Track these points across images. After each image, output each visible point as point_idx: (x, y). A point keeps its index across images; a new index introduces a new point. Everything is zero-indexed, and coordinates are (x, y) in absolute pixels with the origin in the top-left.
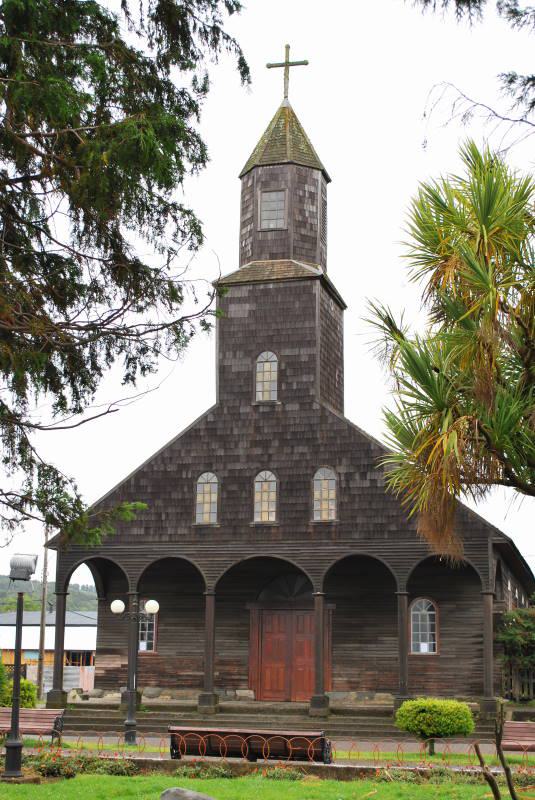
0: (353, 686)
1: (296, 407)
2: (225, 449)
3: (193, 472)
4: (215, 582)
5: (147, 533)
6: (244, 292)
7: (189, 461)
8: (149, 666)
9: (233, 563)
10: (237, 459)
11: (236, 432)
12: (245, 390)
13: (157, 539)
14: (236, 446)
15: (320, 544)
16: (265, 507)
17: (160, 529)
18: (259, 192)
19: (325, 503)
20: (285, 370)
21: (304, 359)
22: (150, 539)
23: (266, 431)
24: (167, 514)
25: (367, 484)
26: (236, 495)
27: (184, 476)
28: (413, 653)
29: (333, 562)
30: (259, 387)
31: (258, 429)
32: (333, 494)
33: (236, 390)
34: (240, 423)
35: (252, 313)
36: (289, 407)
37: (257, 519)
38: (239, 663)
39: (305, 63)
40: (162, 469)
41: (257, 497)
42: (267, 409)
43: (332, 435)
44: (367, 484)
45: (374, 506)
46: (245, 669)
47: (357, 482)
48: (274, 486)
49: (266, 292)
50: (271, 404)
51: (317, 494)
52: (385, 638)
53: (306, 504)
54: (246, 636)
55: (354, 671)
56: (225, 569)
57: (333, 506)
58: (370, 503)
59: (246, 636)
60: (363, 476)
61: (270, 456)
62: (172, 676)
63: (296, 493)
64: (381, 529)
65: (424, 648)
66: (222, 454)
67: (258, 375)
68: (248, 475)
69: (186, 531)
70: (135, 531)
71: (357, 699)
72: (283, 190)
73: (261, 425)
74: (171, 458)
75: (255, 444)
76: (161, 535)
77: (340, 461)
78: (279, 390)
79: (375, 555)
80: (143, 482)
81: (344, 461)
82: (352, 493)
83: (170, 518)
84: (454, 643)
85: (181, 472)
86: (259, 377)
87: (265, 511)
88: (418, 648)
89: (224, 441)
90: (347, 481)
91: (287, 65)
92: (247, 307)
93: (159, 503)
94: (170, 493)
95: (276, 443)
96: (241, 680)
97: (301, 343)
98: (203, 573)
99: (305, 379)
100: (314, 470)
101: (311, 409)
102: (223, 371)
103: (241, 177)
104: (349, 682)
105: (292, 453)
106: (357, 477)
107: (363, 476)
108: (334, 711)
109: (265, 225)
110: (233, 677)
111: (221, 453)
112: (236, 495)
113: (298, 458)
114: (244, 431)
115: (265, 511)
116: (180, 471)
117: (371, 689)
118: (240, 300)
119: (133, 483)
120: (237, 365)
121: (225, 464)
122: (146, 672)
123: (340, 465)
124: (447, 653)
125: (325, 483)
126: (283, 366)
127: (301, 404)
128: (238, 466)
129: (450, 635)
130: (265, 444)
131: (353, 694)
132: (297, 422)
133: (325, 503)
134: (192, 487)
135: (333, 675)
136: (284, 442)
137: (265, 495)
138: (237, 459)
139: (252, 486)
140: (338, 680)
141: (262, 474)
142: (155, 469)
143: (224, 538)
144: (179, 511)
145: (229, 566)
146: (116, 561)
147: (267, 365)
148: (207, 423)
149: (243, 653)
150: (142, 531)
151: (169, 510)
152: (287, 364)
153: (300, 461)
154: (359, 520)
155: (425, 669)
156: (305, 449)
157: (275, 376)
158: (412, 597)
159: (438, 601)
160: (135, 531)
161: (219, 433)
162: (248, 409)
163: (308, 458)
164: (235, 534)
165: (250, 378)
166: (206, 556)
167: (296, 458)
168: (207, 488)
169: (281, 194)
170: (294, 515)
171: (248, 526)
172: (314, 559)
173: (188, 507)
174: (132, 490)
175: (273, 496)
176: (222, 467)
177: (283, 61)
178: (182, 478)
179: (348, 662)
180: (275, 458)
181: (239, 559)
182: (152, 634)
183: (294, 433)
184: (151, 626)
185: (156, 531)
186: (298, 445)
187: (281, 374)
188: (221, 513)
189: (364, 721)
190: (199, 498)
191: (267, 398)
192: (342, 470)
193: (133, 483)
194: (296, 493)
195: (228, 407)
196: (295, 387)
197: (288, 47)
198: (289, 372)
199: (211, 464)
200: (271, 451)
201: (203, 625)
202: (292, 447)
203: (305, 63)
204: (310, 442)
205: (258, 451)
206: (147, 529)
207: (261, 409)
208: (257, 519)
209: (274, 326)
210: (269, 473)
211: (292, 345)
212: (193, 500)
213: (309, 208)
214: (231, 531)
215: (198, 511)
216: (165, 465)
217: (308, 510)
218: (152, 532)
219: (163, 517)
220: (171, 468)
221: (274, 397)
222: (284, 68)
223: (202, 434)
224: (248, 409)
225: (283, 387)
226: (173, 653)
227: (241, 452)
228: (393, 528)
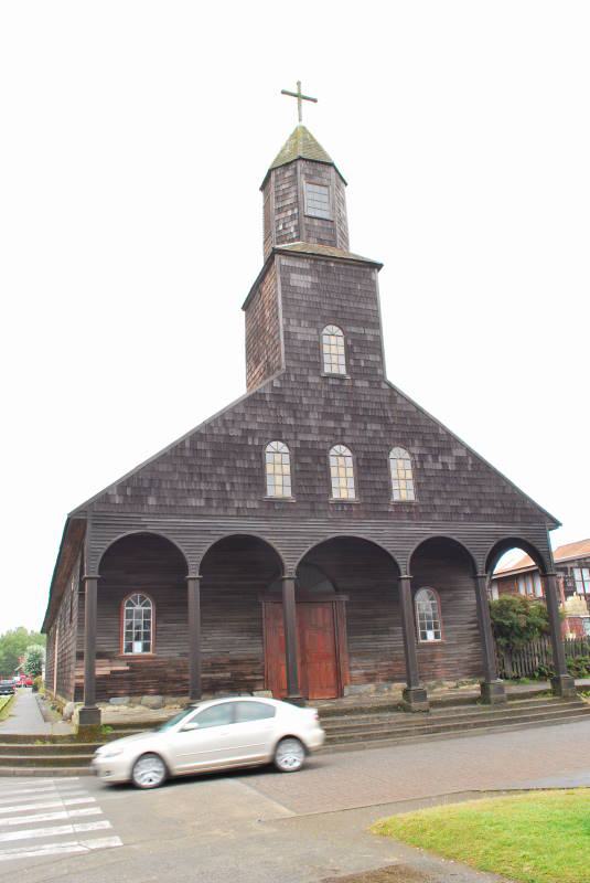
0: (370, 678)
1: (366, 384)
2: (295, 417)
3: (260, 439)
4: (296, 564)
5: (209, 506)
6: (304, 265)
7: (254, 426)
8: (145, 670)
9: (315, 543)
10: (308, 430)
11: (305, 401)
12: (312, 359)
13: (222, 513)
14: (307, 417)
15: (404, 525)
16: (343, 483)
17: (225, 502)
19: (402, 482)
20: (352, 346)
21: (370, 338)
22: (213, 512)
23: (337, 404)
24: (232, 484)
25: (440, 467)
26: (311, 470)
27: (250, 443)
28: (421, 641)
29: (417, 544)
31: (328, 401)
32: (409, 475)
33: (302, 358)
34: (309, 393)
35: (315, 286)
36: (358, 383)
37: (335, 495)
38: (253, 661)
40: (224, 432)
41: (334, 472)
42: (337, 382)
43: (403, 415)
44: (440, 467)
45: (448, 488)
46: (259, 667)
47: (430, 464)
48: (349, 461)
49: (328, 269)
50: (341, 378)
51: (394, 474)
52: (395, 628)
53: (386, 482)
54: (258, 632)
55: (370, 663)
56: (307, 550)
57: (411, 485)
58: (444, 485)
59: (258, 632)
60: (435, 458)
61: (343, 429)
62: (175, 681)
63: (371, 469)
64: (456, 511)
65: (430, 636)
66: (292, 423)
68: (321, 447)
69: (256, 505)
70: (194, 502)
71: (377, 691)
73: (332, 397)
74: (233, 421)
75: (326, 416)
76: (226, 508)
77: (413, 441)
78: (347, 365)
79: (454, 537)
80: (201, 446)
81: (416, 442)
82: (429, 474)
83: (237, 489)
84: (455, 630)
85: (247, 438)
86: (326, 349)
87: (343, 484)
88: (424, 636)
89: (293, 409)
90: (422, 462)
91: (299, 96)
92: (310, 279)
93: (222, 471)
94: (234, 460)
95: (348, 418)
96: (255, 680)
98: (281, 553)
99: (371, 358)
100: (389, 448)
101: (380, 388)
104: (366, 674)
105: (365, 429)
106: (430, 459)
107: (435, 458)
108: (435, 704)
109: (311, 212)
110: (248, 678)
111: (290, 421)
112: (311, 470)
113: (371, 435)
114: (313, 402)
115: (343, 484)
116: (244, 437)
117: (386, 680)
118: (302, 271)
119: (187, 444)
121: (296, 433)
122: (144, 678)
123: (413, 445)
124: (449, 639)
125: (400, 463)
126: (350, 342)
127: (370, 382)
128: (310, 438)
129: (450, 623)
130: (338, 418)
131: (371, 687)
132: (368, 398)
133: (402, 482)
134: (261, 454)
135: (350, 668)
136: (356, 418)
137: (342, 471)
138: (308, 430)
139: (326, 458)
140: (355, 673)
141: (337, 447)
142: (216, 432)
143: (302, 514)
144: (246, 481)
145: (310, 546)
146: (170, 538)
148: (273, 388)
149: (256, 650)
150: (202, 503)
151: (235, 481)
152: (353, 340)
153: (374, 438)
154: (437, 502)
155: (433, 656)
156: (375, 427)
157: (342, 350)
158: (415, 588)
159: (440, 590)
160: (194, 502)
161: (287, 400)
162: (317, 380)
163: (382, 435)
164: (313, 510)
165: (317, 348)
166: (283, 534)
167: (370, 434)
168: (278, 458)
169: (324, 190)
170: (374, 493)
171: (327, 502)
172: (400, 540)
173: (257, 478)
174: (187, 453)
175: (350, 472)
176: (292, 436)
178: (246, 444)
179: (363, 654)
180: (348, 433)
181: (322, 539)
182: (149, 633)
183: (365, 409)
184: (147, 624)
185: (218, 503)
186: (371, 422)
188: (295, 486)
189: (465, 711)
190: (269, 469)
191: (335, 370)
192: (416, 451)
193: (187, 444)
194: (371, 469)
195: (295, 375)
197: (299, 84)
198: (355, 349)
199: (280, 432)
200: (344, 425)
201: (186, 620)
202: (365, 423)
204: (383, 420)
205: (331, 424)
206: (208, 499)
207: (331, 382)
208: (335, 495)
209: (337, 302)
210: (343, 448)
212: (263, 468)
214: (308, 506)
215: (269, 480)
216: (227, 428)
217: (387, 489)
218: (215, 504)
219: (228, 488)
220: (235, 432)
221: (343, 371)
223: (268, 399)
224: (317, 380)
226: (175, 654)
227: (313, 423)
228: (468, 511)
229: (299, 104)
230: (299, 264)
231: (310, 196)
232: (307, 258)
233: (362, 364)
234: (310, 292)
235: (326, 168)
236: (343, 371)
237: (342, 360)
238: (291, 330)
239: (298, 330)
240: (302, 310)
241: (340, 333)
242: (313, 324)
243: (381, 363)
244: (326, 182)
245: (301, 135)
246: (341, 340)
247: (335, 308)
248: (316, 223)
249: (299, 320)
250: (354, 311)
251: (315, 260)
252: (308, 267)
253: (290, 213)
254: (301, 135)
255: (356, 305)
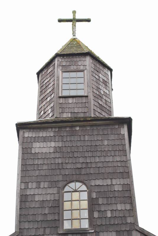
6: (50, 133)
12: (50, 218)
18: (61, 72)
20: (97, 199)
30: (67, 215)
33: (40, 218)
35: (57, 150)
39: (88, 20)
67: (65, 203)
72: (83, 71)
78: (91, 218)
91: (74, 21)
92: (53, 144)
97: (112, 175)
102: (23, 199)
103: (38, 74)
109: (66, 93)
118: (45, 139)
120: (42, 194)
147: (76, 196)
157: (85, 204)
165: (57, 206)
169: (80, 74)
177: (71, 17)
187: (93, 204)
191: (76, 225)
196: (109, 215)
197: (74, 12)
198: (100, 201)
203: (88, 20)
209: (81, 160)
211: (100, 175)
213: (103, 89)
222: (71, 23)
225: (96, 215)
229: (74, 26)
230: (43, 134)
231: (65, 81)
232: (52, 128)
233: (109, 215)
234: (53, 156)
235: (106, 70)
236: (85, 225)
237: (85, 214)
238: (28, 192)
239: (37, 191)
240: (43, 173)
241: (84, 188)
242: (53, 184)
243: (132, 211)
244: (82, 68)
245: (74, 42)
246: (85, 196)
247: (79, 166)
248: (70, 100)
249: (39, 183)
250: (99, 165)
251: (59, 128)
252: (52, 135)
253: (48, 99)
254: (74, 42)
255: (102, 159)
